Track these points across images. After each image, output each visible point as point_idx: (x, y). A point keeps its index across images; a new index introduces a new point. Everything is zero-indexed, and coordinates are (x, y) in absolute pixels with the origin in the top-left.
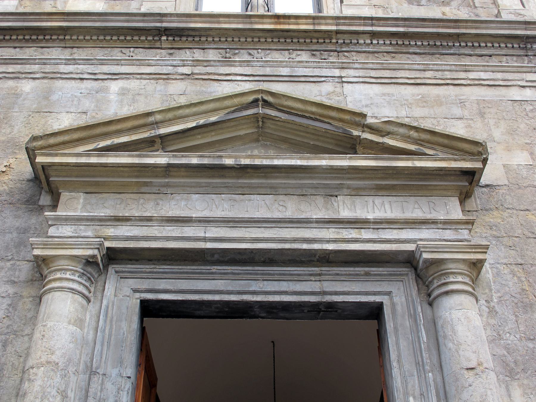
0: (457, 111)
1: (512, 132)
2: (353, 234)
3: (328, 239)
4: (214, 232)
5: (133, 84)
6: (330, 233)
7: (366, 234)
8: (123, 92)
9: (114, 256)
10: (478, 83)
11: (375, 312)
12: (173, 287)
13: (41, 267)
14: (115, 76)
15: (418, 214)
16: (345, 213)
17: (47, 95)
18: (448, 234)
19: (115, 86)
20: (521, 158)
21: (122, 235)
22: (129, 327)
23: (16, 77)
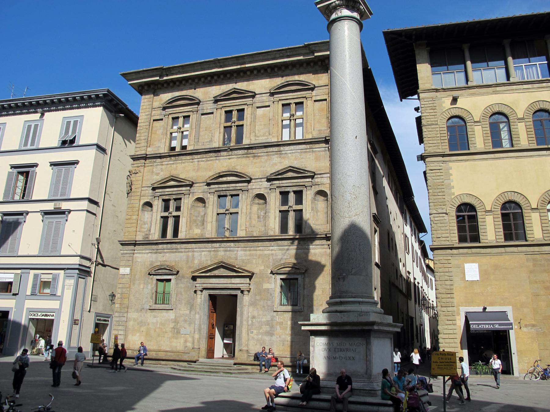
0: (255, 257)
1: (263, 262)
2: (233, 285)
3: (230, 286)
4: (216, 285)
5: (206, 253)
6: (230, 285)
7: (235, 285)
8: (204, 255)
9: (204, 289)
10: (260, 250)
11: (236, 296)
12: (212, 292)
13: (195, 292)
14: (203, 251)
15: (242, 282)
16: (233, 282)
17: (193, 256)
18: (246, 285)
19: (203, 253)
20: (262, 268)
21: (205, 286)
22: (207, 297)
23: (188, 252)
